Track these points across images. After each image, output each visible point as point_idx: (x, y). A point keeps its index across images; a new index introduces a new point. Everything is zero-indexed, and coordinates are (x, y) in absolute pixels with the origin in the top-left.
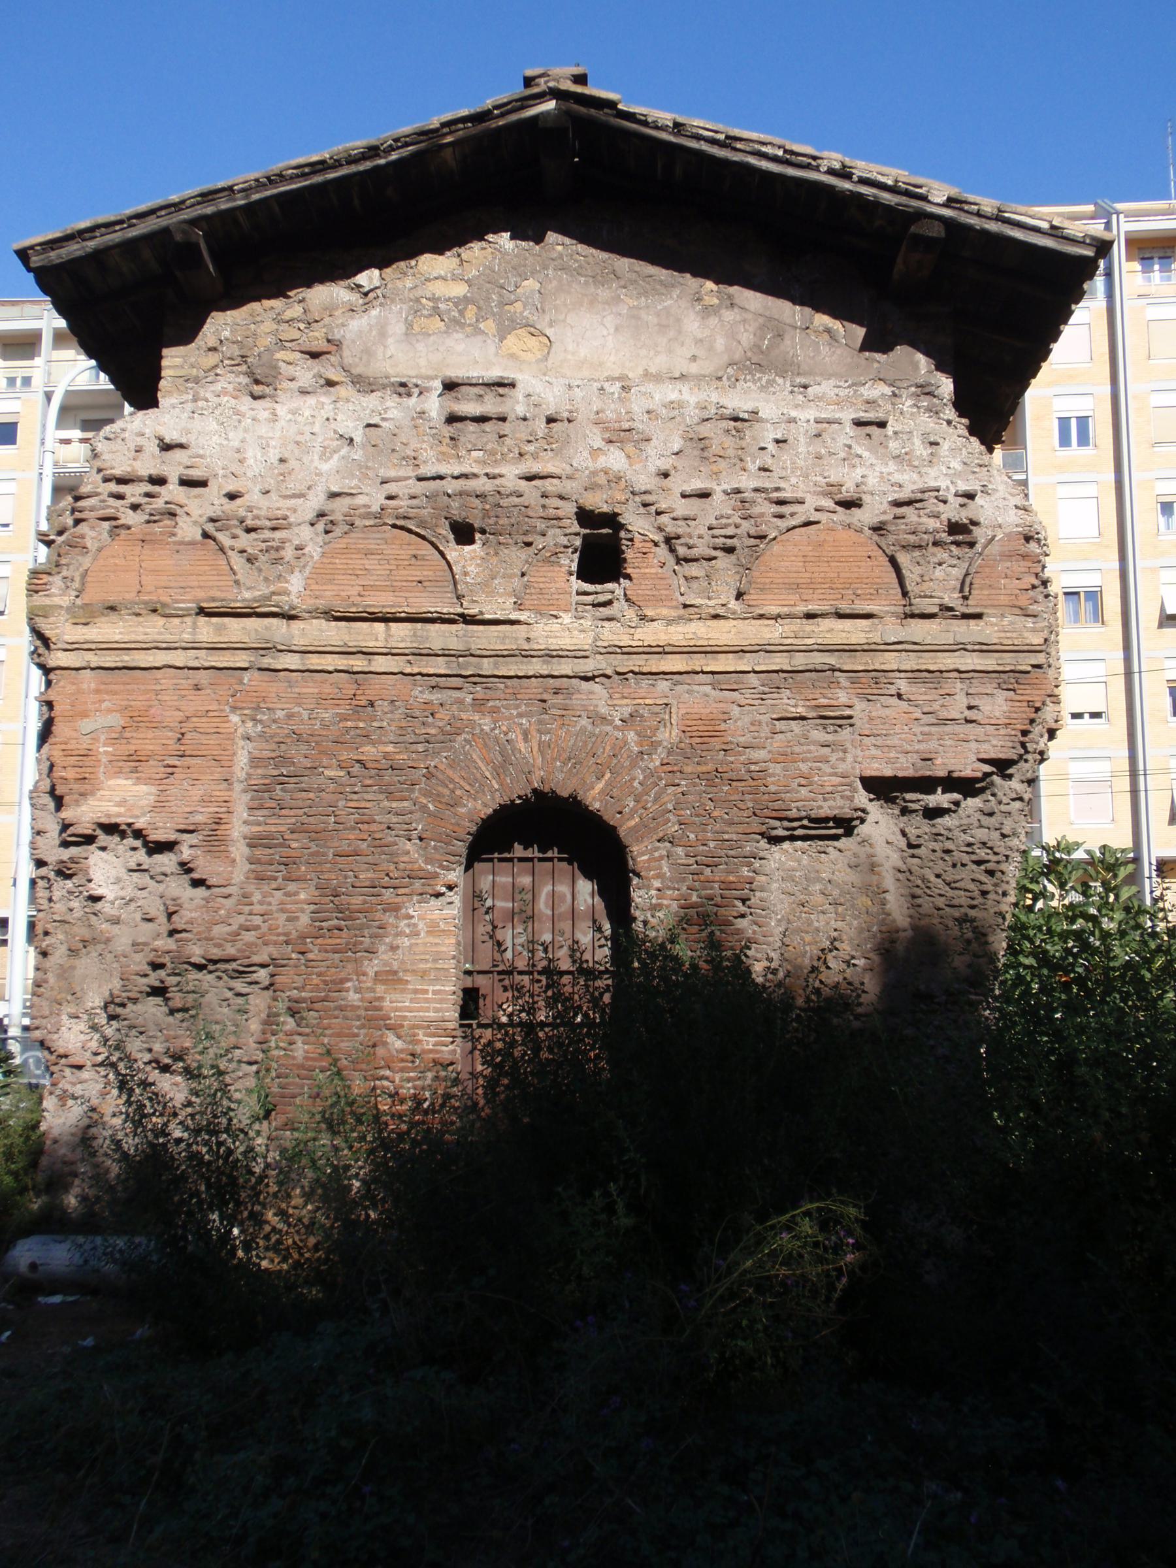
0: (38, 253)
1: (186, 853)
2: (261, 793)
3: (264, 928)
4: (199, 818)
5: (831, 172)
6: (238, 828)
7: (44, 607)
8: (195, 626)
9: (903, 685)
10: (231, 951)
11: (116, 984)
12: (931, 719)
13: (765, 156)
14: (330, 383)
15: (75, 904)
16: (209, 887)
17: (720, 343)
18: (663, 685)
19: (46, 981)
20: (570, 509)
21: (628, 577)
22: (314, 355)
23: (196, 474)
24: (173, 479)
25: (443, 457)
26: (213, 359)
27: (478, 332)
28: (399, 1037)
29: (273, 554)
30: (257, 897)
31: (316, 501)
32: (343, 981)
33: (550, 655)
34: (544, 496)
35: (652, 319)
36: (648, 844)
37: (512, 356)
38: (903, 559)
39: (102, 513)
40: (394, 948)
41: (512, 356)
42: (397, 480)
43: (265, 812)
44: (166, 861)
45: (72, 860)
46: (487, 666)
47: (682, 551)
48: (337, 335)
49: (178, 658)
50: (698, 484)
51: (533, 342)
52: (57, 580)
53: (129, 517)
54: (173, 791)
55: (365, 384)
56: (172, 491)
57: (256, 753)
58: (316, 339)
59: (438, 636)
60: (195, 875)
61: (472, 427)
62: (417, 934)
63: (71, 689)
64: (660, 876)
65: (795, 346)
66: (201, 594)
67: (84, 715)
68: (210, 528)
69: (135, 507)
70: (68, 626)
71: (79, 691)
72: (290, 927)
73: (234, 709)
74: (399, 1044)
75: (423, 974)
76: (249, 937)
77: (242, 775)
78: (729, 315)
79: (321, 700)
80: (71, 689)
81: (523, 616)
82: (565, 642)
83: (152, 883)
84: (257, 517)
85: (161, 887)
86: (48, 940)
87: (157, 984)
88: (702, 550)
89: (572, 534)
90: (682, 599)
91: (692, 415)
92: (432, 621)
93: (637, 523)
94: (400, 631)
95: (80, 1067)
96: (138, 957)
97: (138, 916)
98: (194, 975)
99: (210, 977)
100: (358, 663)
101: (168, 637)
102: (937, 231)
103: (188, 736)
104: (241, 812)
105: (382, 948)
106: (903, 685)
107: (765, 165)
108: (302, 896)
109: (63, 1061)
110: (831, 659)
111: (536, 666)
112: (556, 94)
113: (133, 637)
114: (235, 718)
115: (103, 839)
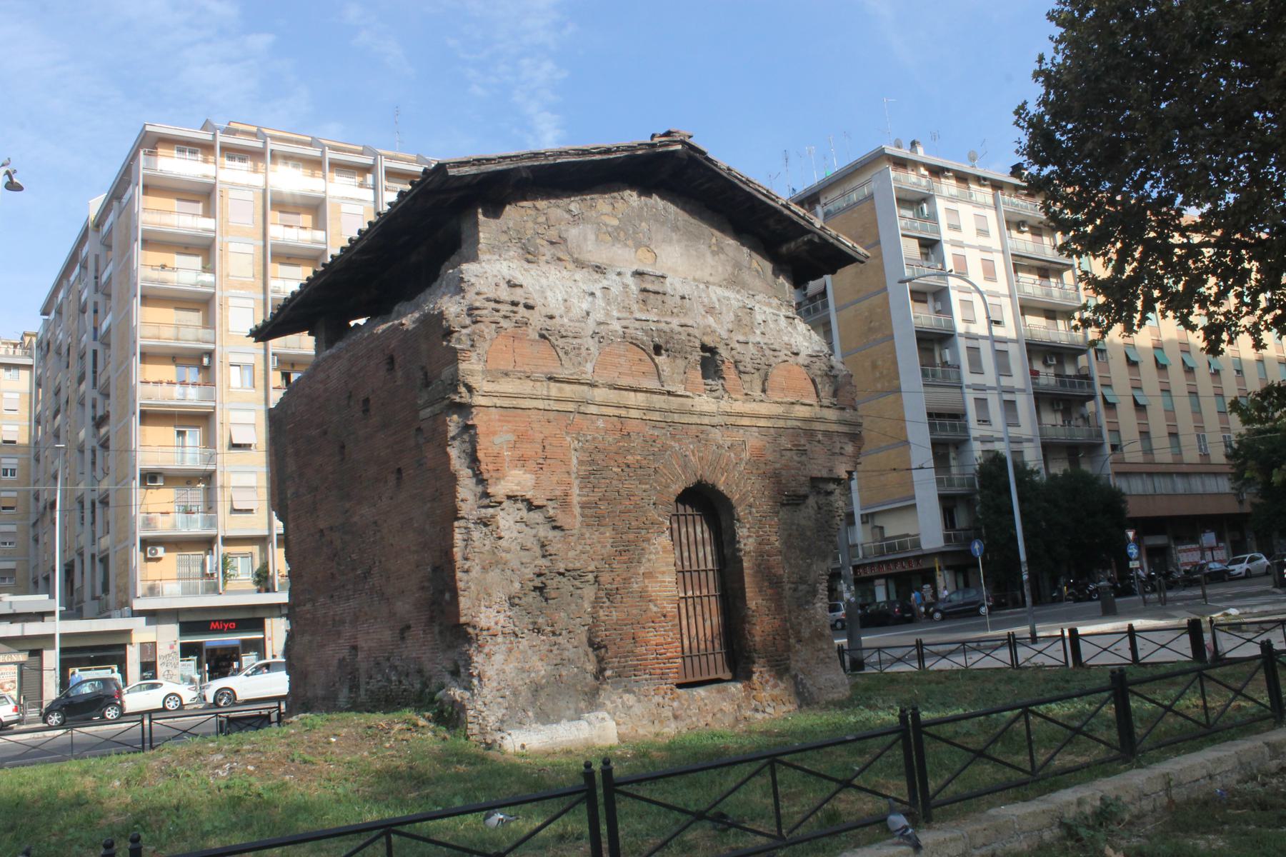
0: (454, 167)
1: (551, 512)
2: (585, 479)
3: (592, 552)
4: (558, 493)
5: (782, 205)
6: (576, 497)
7: (471, 371)
8: (548, 388)
9: (820, 437)
10: (578, 565)
11: (517, 585)
12: (829, 453)
13: (759, 192)
14: (559, 259)
15: (487, 542)
16: (563, 530)
17: (720, 269)
18: (741, 431)
19: (469, 588)
20: (698, 344)
21: (724, 378)
22: (552, 243)
23: (530, 302)
24: (521, 306)
25: (641, 310)
26: (504, 238)
27: (626, 245)
28: (655, 605)
29: (577, 351)
30: (587, 535)
31: (591, 325)
32: (630, 578)
33: (702, 414)
34: (689, 335)
35: (694, 253)
36: (743, 507)
37: (640, 260)
38: (818, 380)
39: (492, 319)
40: (649, 560)
41: (640, 260)
42: (625, 319)
43: (587, 490)
44: (536, 516)
45: (493, 517)
46: (676, 418)
47: (742, 368)
48: (564, 235)
49: (540, 404)
50: (742, 338)
51: (649, 255)
52: (474, 355)
53: (504, 323)
54: (542, 477)
55: (580, 264)
56: (521, 309)
57: (581, 458)
58: (553, 234)
59: (659, 401)
60: (558, 524)
61: (652, 296)
62: (658, 553)
63: (485, 418)
64: (748, 522)
65: (746, 276)
66: (546, 370)
67: (494, 433)
68: (544, 332)
69: (506, 317)
70: (485, 383)
71: (490, 420)
72: (603, 551)
73: (568, 433)
74: (655, 609)
75: (663, 573)
76: (584, 556)
77: (575, 470)
78: (722, 256)
79: (606, 431)
80: (485, 418)
81: (688, 394)
82: (706, 408)
83: (527, 530)
84: (566, 331)
85: (534, 531)
86: (467, 564)
87: (540, 585)
88: (749, 369)
89: (697, 356)
90: (746, 391)
91: (735, 304)
92: (655, 393)
93: (723, 352)
94: (641, 396)
95: (495, 635)
96: (527, 571)
97: (518, 548)
98: (560, 578)
99: (564, 580)
100: (623, 412)
101: (535, 392)
102: (816, 240)
103: (547, 447)
104: (575, 491)
105: (644, 560)
106: (820, 437)
107: (760, 196)
108: (608, 534)
109: (485, 633)
110: (799, 424)
111: (695, 419)
112: (683, 142)
113: (519, 391)
114: (568, 439)
115: (506, 504)
